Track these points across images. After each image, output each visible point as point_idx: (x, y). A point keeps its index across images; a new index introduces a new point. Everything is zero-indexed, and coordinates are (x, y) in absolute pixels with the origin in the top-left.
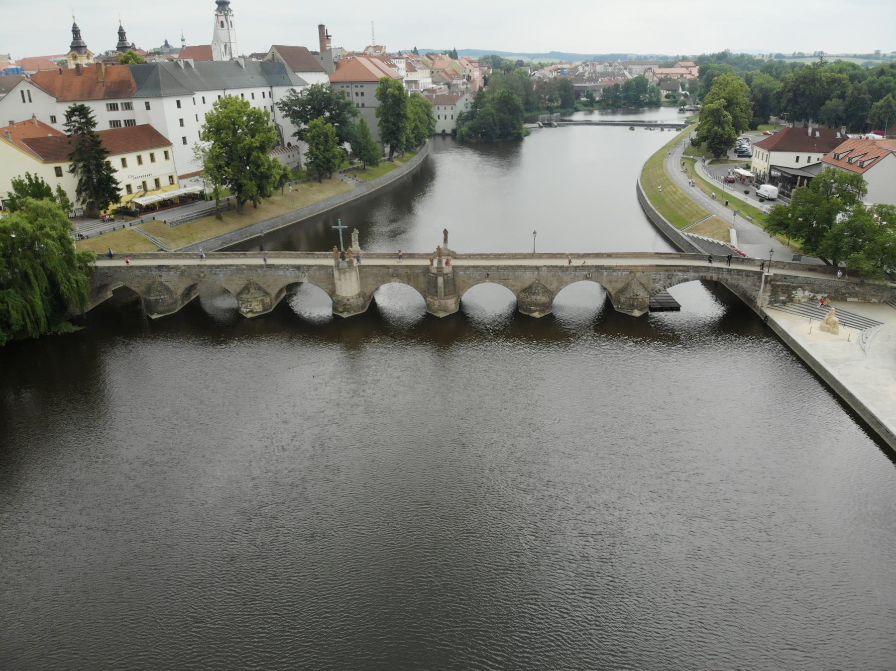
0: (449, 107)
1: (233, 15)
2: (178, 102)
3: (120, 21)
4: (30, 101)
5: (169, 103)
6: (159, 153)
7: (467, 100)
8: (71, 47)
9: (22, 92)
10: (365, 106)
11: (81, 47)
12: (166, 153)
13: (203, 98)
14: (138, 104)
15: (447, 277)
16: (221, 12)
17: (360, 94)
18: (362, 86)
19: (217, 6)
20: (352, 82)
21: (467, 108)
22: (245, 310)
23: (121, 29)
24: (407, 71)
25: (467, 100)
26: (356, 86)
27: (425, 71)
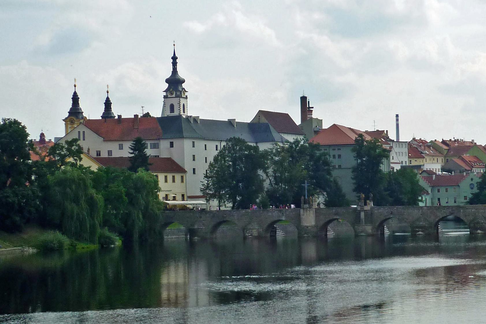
0: (451, 190)
1: (186, 98)
2: (193, 142)
3: (108, 92)
4: (84, 140)
5: (187, 143)
6: (178, 177)
7: (472, 179)
8: (69, 112)
9: (79, 132)
10: (342, 167)
11: (79, 112)
12: (182, 177)
13: (205, 145)
14: (164, 144)
15: (367, 212)
16: (172, 94)
17: (337, 157)
18: (339, 149)
19: (166, 85)
20: (330, 146)
21: (472, 188)
22: (247, 234)
23: (108, 100)
24: (409, 157)
25: (472, 179)
26: (334, 150)
27: (436, 159)
